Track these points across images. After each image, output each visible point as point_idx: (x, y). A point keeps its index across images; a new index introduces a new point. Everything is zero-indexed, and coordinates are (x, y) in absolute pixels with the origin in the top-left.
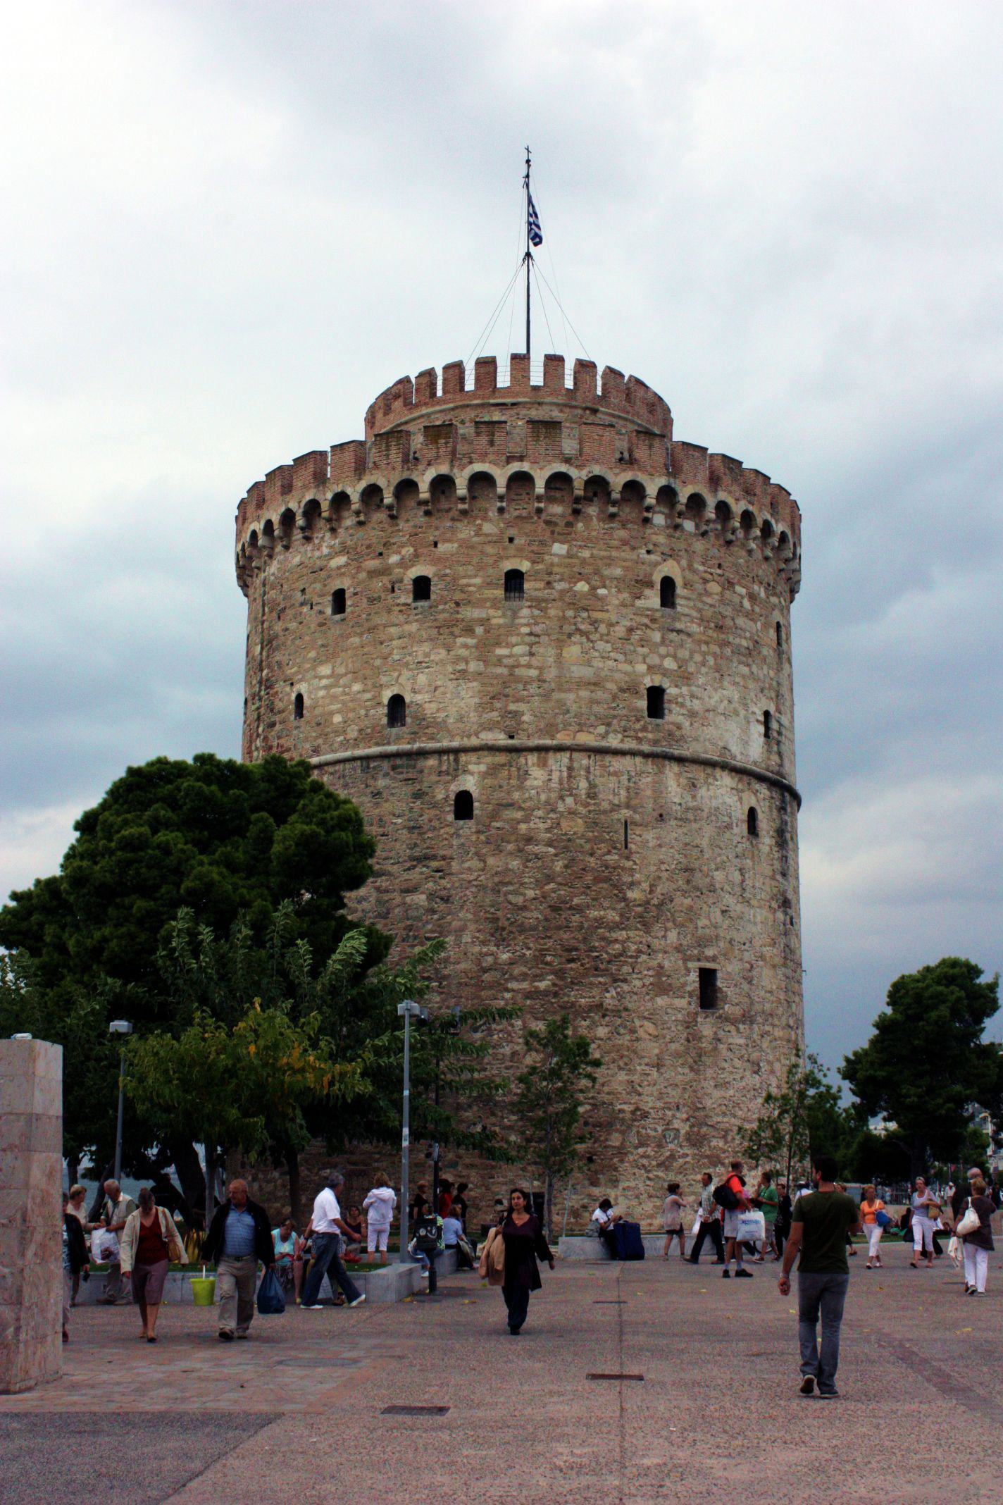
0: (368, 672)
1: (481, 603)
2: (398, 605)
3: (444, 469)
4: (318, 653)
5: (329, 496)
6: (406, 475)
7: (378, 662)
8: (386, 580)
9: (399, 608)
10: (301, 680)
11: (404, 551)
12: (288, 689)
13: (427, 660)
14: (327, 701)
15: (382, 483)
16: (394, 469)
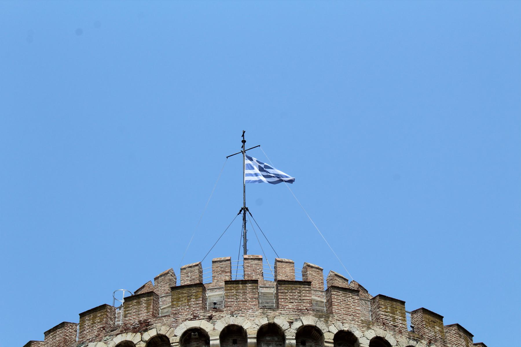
16: (400, 332)
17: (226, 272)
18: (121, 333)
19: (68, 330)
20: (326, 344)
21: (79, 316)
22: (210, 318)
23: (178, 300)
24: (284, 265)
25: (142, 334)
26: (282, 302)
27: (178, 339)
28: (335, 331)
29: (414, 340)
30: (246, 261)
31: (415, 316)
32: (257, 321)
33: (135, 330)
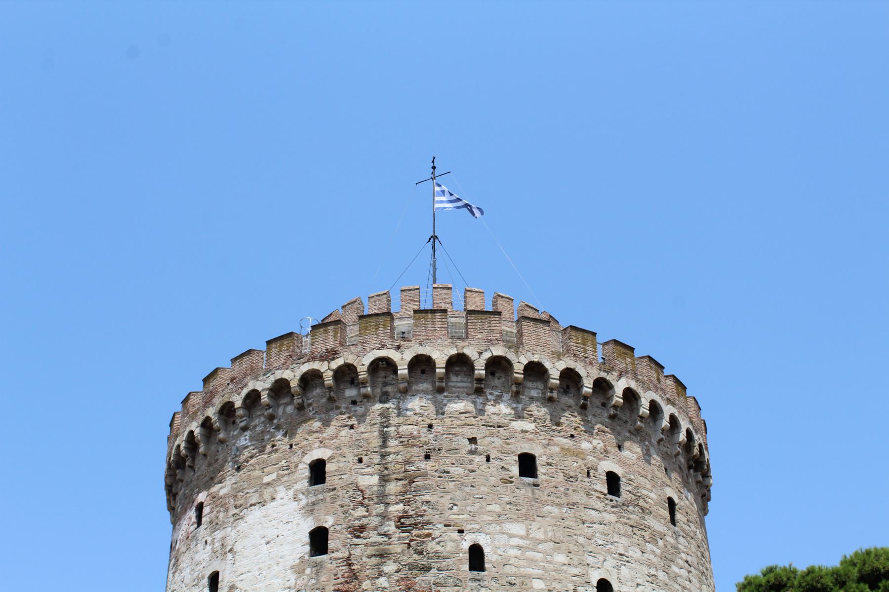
0: (572, 547)
1: (658, 517)
2: (596, 491)
3: (633, 385)
4: (504, 509)
5: (525, 362)
6: (603, 375)
7: (581, 540)
8: (581, 462)
9: (599, 495)
10: (478, 531)
11: (595, 442)
12: (456, 535)
13: (627, 554)
14: (521, 562)
15: (582, 372)
16: (591, 364)
17: (415, 301)
18: (308, 361)
19: (254, 358)
20: (516, 375)
21: (266, 344)
22: (398, 347)
23: (366, 328)
24: (474, 295)
25: (329, 363)
26: (471, 332)
27: (365, 368)
28: (525, 362)
29: (605, 371)
30: (435, 290)
31: (606, 347)
32: (446, 351)
33: (322, 359)
